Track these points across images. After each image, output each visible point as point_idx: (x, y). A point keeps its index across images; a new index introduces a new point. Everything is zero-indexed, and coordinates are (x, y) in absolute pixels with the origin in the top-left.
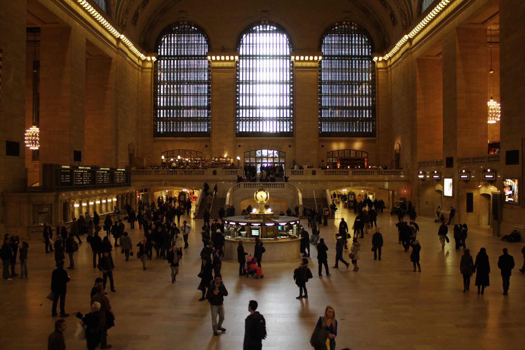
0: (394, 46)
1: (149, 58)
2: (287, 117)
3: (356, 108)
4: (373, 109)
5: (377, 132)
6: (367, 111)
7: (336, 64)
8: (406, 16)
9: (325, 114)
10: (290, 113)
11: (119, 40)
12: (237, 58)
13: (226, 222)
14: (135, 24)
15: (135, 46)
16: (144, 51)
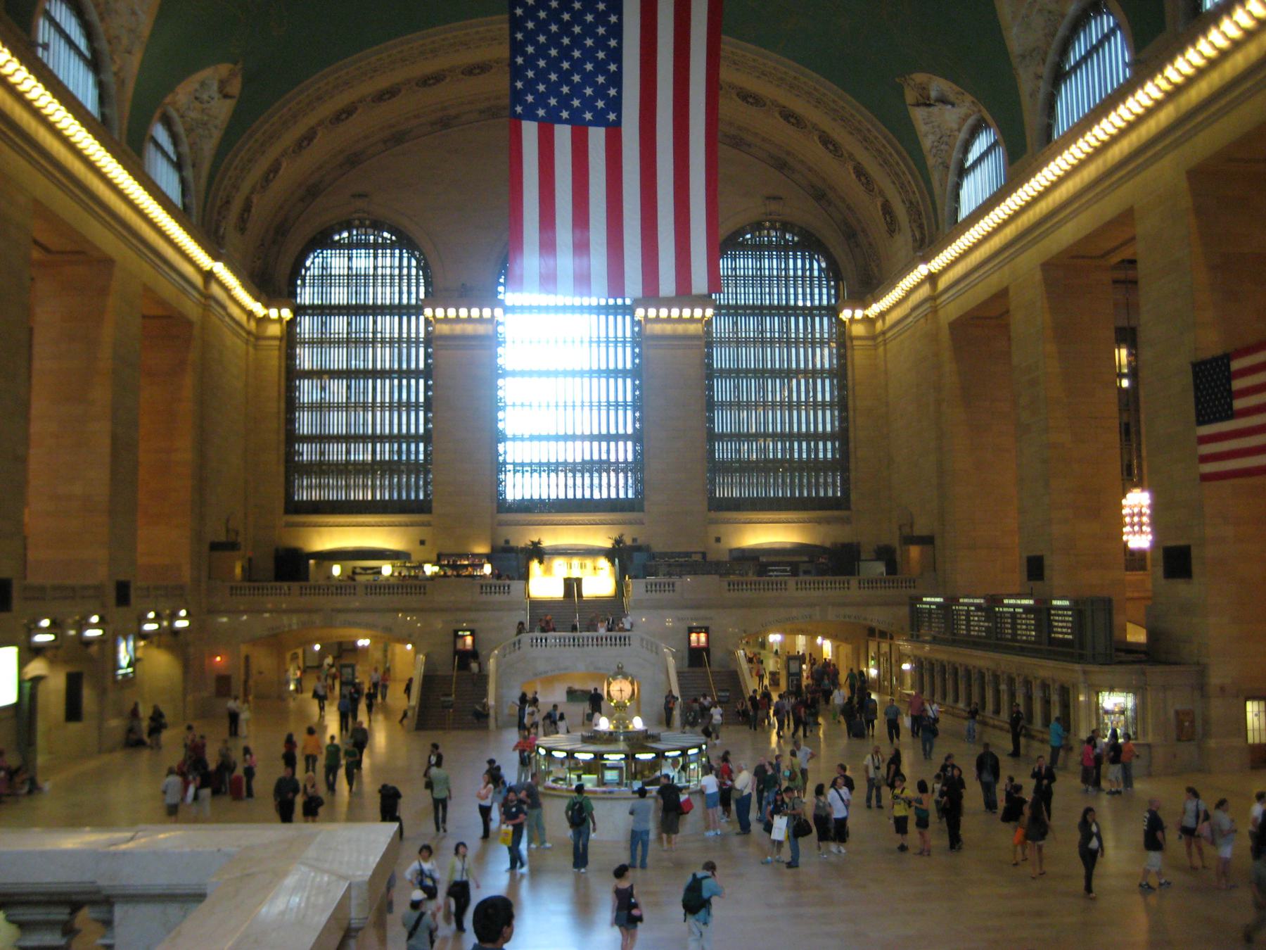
0: (892, 286)
1: (273, 313)
2: (626, 461)
3: (800, 437)
4: (842, 436)
5: (853, 497)
6: (829, 445)
7: (749, 326)
8: (920, 214)
9: (723, 451)
10: (635, 451)
11: (209, 276)
12: (498, 312)
13: (542, 751)
14: (242, 230)
15: (244, 286)
16: (264, 296)
